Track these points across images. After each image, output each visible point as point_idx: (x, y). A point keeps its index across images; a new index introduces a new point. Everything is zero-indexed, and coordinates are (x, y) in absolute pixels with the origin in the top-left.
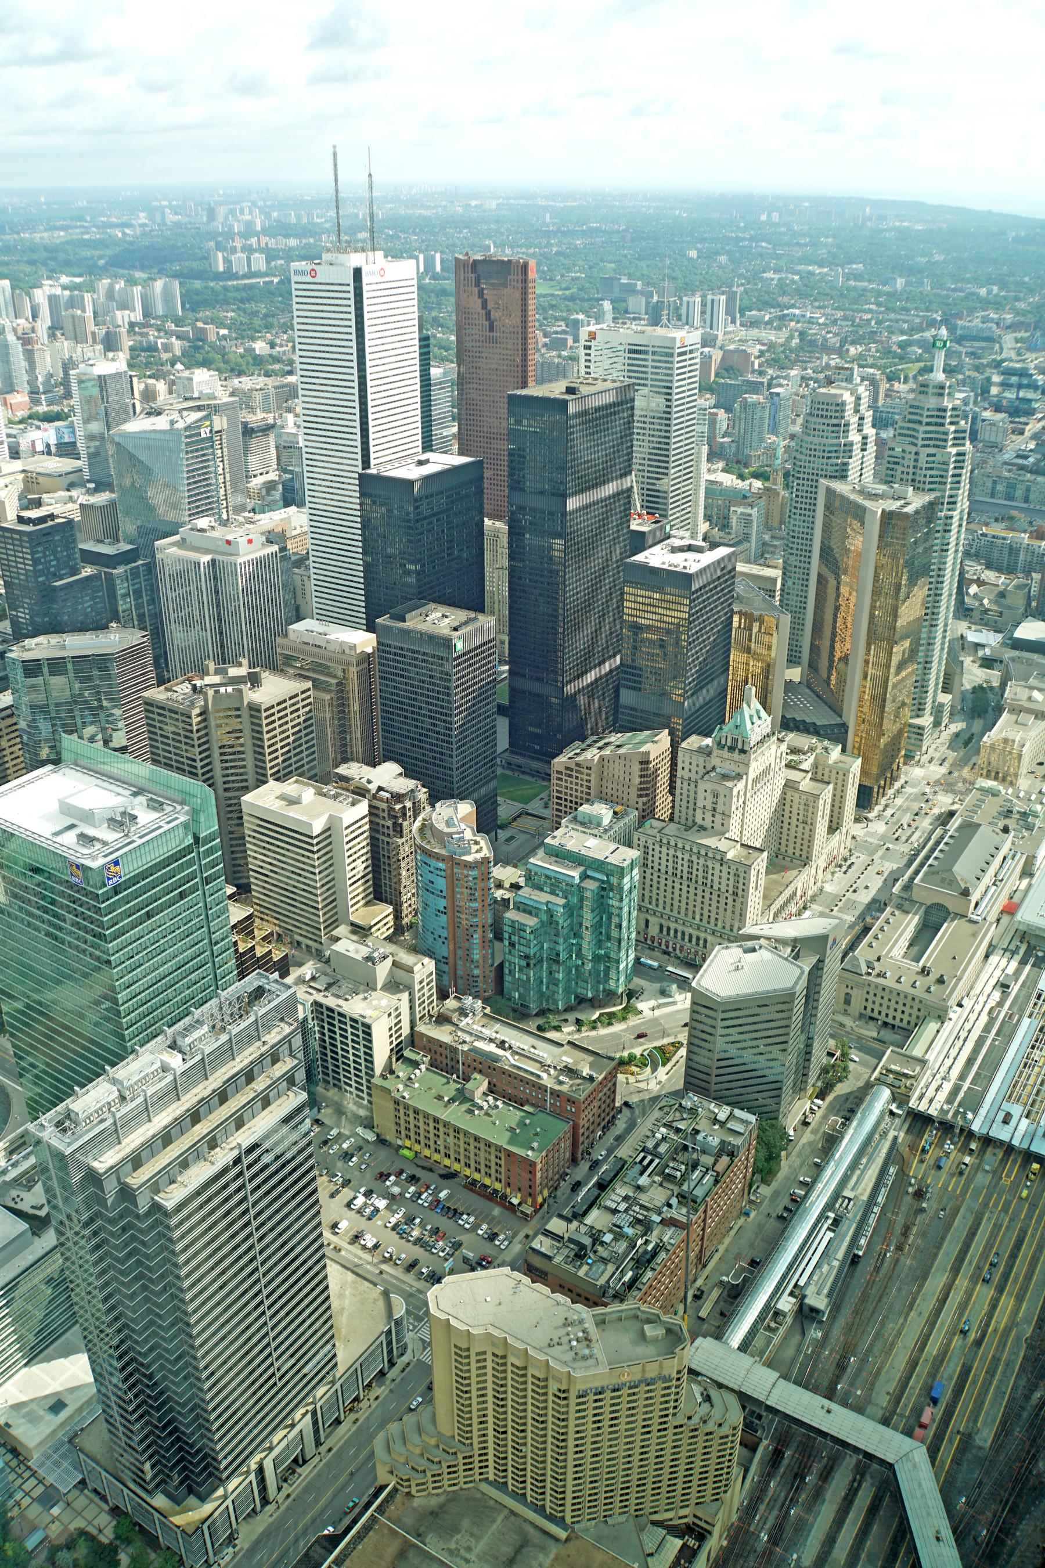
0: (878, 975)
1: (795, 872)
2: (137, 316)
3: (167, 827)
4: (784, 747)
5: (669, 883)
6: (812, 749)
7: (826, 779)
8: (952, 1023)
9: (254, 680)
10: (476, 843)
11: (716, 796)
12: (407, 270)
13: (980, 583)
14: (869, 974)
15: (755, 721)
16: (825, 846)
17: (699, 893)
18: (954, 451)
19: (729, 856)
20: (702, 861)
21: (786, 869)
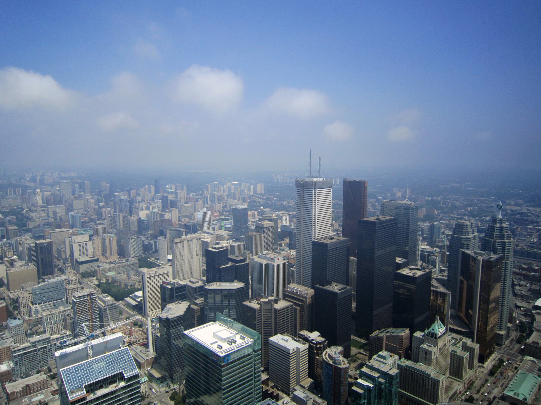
2: (252, 193)
3: (245, 345)
4: (450, 338)
9: (276, 301)
10: (343, 361)
11: (426, 354)
15: (439, 328)
18: (507, 241)
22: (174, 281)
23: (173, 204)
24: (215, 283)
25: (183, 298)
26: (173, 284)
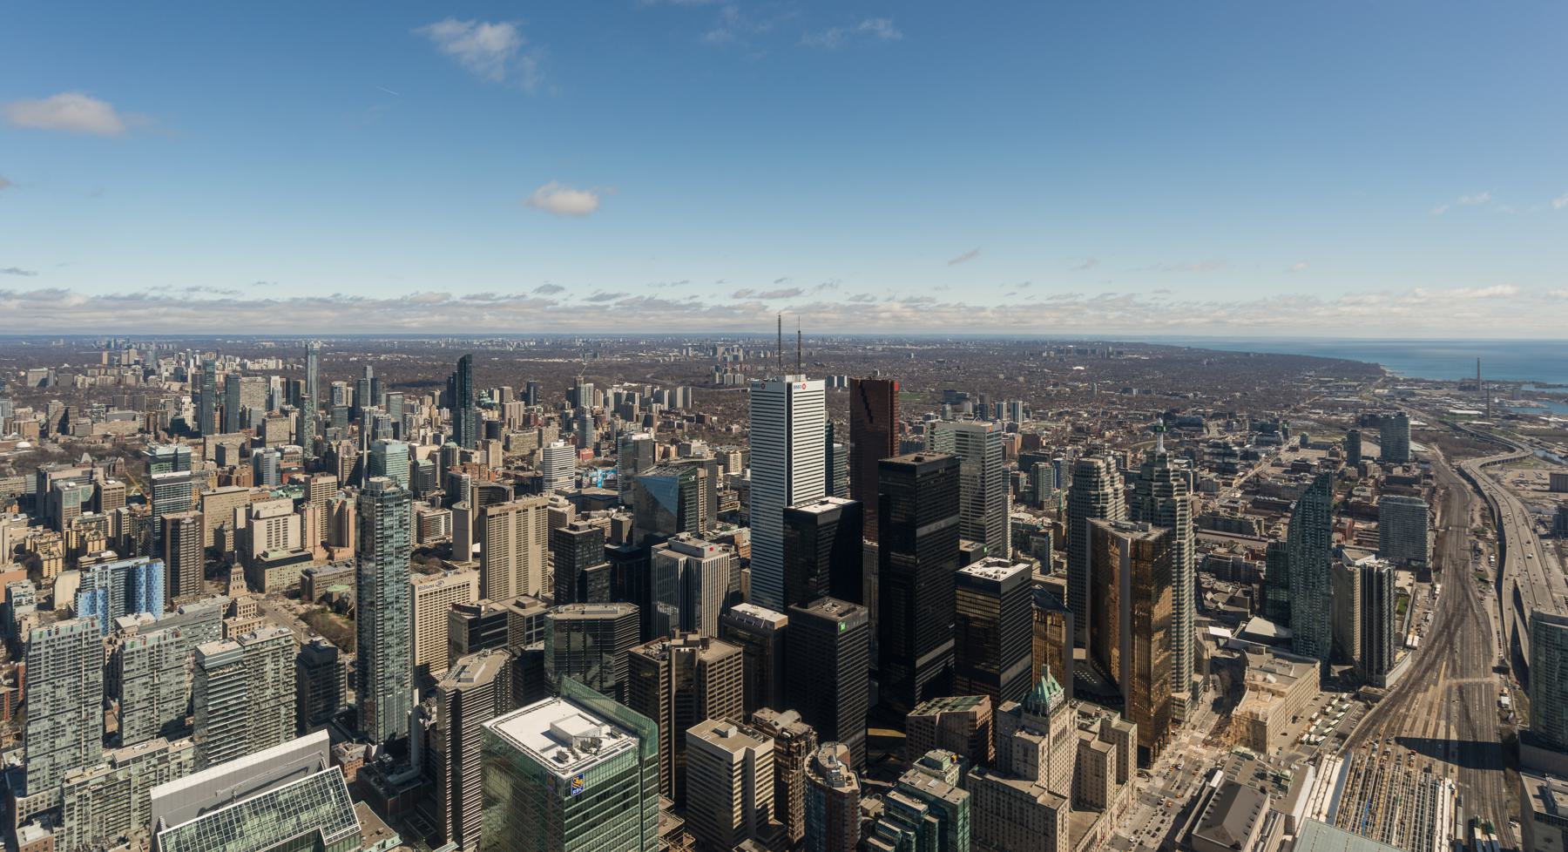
4: (1075, 713)
6: (1097, 715)
9: (705, 643)
12: (820, 385)
13: (1214, 591)
15: (1052, 692)
22: (482, 602)
23: (492, 430)
24: (570, 606)
25: (496, 641)
26: (477, 610)
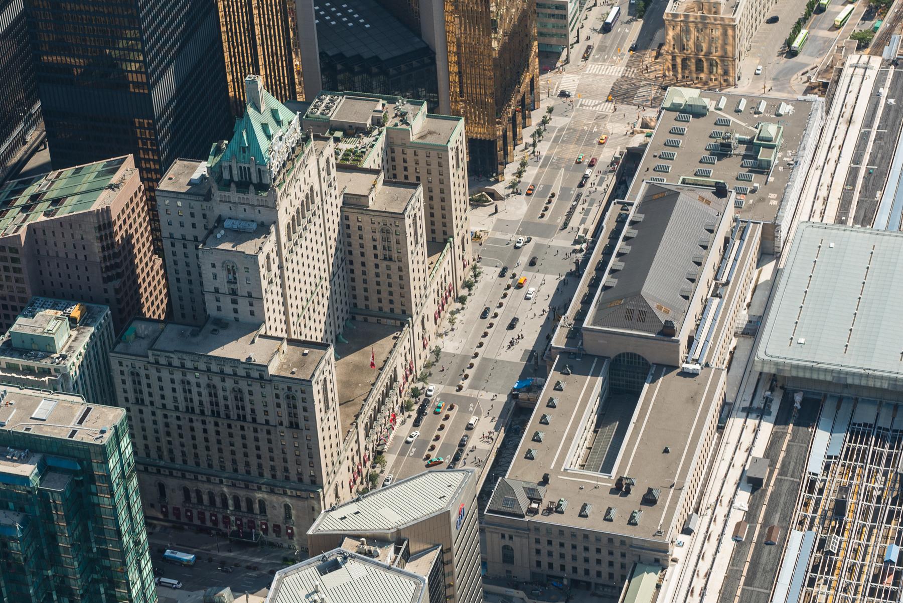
0: (549, 511)
1: (386, 343)
5: (184, 423)
7: (412, 179)
8: (678, 566)
14: (534, 512)
16: (426, 276)
17: (236, 431)
19: (272, 370)
20: (229, 384)
21: (371, 339)
